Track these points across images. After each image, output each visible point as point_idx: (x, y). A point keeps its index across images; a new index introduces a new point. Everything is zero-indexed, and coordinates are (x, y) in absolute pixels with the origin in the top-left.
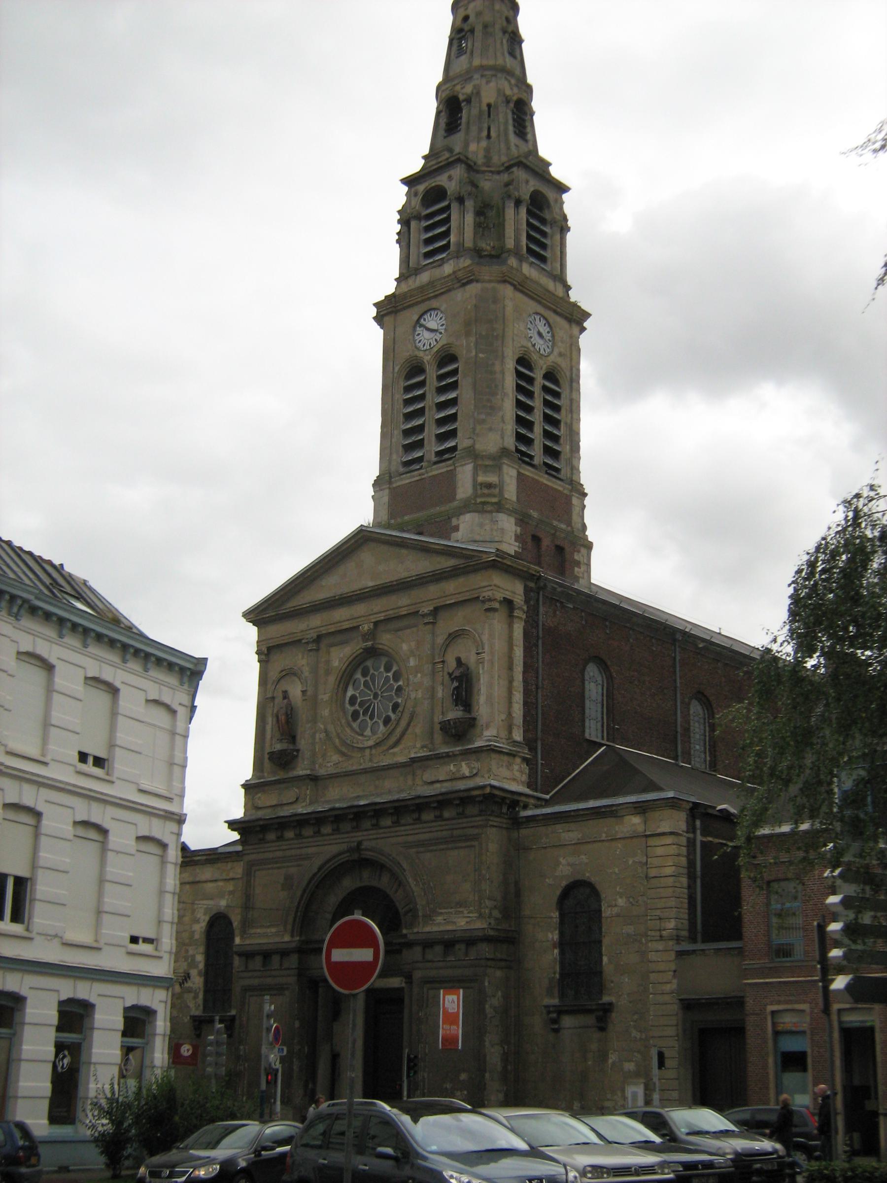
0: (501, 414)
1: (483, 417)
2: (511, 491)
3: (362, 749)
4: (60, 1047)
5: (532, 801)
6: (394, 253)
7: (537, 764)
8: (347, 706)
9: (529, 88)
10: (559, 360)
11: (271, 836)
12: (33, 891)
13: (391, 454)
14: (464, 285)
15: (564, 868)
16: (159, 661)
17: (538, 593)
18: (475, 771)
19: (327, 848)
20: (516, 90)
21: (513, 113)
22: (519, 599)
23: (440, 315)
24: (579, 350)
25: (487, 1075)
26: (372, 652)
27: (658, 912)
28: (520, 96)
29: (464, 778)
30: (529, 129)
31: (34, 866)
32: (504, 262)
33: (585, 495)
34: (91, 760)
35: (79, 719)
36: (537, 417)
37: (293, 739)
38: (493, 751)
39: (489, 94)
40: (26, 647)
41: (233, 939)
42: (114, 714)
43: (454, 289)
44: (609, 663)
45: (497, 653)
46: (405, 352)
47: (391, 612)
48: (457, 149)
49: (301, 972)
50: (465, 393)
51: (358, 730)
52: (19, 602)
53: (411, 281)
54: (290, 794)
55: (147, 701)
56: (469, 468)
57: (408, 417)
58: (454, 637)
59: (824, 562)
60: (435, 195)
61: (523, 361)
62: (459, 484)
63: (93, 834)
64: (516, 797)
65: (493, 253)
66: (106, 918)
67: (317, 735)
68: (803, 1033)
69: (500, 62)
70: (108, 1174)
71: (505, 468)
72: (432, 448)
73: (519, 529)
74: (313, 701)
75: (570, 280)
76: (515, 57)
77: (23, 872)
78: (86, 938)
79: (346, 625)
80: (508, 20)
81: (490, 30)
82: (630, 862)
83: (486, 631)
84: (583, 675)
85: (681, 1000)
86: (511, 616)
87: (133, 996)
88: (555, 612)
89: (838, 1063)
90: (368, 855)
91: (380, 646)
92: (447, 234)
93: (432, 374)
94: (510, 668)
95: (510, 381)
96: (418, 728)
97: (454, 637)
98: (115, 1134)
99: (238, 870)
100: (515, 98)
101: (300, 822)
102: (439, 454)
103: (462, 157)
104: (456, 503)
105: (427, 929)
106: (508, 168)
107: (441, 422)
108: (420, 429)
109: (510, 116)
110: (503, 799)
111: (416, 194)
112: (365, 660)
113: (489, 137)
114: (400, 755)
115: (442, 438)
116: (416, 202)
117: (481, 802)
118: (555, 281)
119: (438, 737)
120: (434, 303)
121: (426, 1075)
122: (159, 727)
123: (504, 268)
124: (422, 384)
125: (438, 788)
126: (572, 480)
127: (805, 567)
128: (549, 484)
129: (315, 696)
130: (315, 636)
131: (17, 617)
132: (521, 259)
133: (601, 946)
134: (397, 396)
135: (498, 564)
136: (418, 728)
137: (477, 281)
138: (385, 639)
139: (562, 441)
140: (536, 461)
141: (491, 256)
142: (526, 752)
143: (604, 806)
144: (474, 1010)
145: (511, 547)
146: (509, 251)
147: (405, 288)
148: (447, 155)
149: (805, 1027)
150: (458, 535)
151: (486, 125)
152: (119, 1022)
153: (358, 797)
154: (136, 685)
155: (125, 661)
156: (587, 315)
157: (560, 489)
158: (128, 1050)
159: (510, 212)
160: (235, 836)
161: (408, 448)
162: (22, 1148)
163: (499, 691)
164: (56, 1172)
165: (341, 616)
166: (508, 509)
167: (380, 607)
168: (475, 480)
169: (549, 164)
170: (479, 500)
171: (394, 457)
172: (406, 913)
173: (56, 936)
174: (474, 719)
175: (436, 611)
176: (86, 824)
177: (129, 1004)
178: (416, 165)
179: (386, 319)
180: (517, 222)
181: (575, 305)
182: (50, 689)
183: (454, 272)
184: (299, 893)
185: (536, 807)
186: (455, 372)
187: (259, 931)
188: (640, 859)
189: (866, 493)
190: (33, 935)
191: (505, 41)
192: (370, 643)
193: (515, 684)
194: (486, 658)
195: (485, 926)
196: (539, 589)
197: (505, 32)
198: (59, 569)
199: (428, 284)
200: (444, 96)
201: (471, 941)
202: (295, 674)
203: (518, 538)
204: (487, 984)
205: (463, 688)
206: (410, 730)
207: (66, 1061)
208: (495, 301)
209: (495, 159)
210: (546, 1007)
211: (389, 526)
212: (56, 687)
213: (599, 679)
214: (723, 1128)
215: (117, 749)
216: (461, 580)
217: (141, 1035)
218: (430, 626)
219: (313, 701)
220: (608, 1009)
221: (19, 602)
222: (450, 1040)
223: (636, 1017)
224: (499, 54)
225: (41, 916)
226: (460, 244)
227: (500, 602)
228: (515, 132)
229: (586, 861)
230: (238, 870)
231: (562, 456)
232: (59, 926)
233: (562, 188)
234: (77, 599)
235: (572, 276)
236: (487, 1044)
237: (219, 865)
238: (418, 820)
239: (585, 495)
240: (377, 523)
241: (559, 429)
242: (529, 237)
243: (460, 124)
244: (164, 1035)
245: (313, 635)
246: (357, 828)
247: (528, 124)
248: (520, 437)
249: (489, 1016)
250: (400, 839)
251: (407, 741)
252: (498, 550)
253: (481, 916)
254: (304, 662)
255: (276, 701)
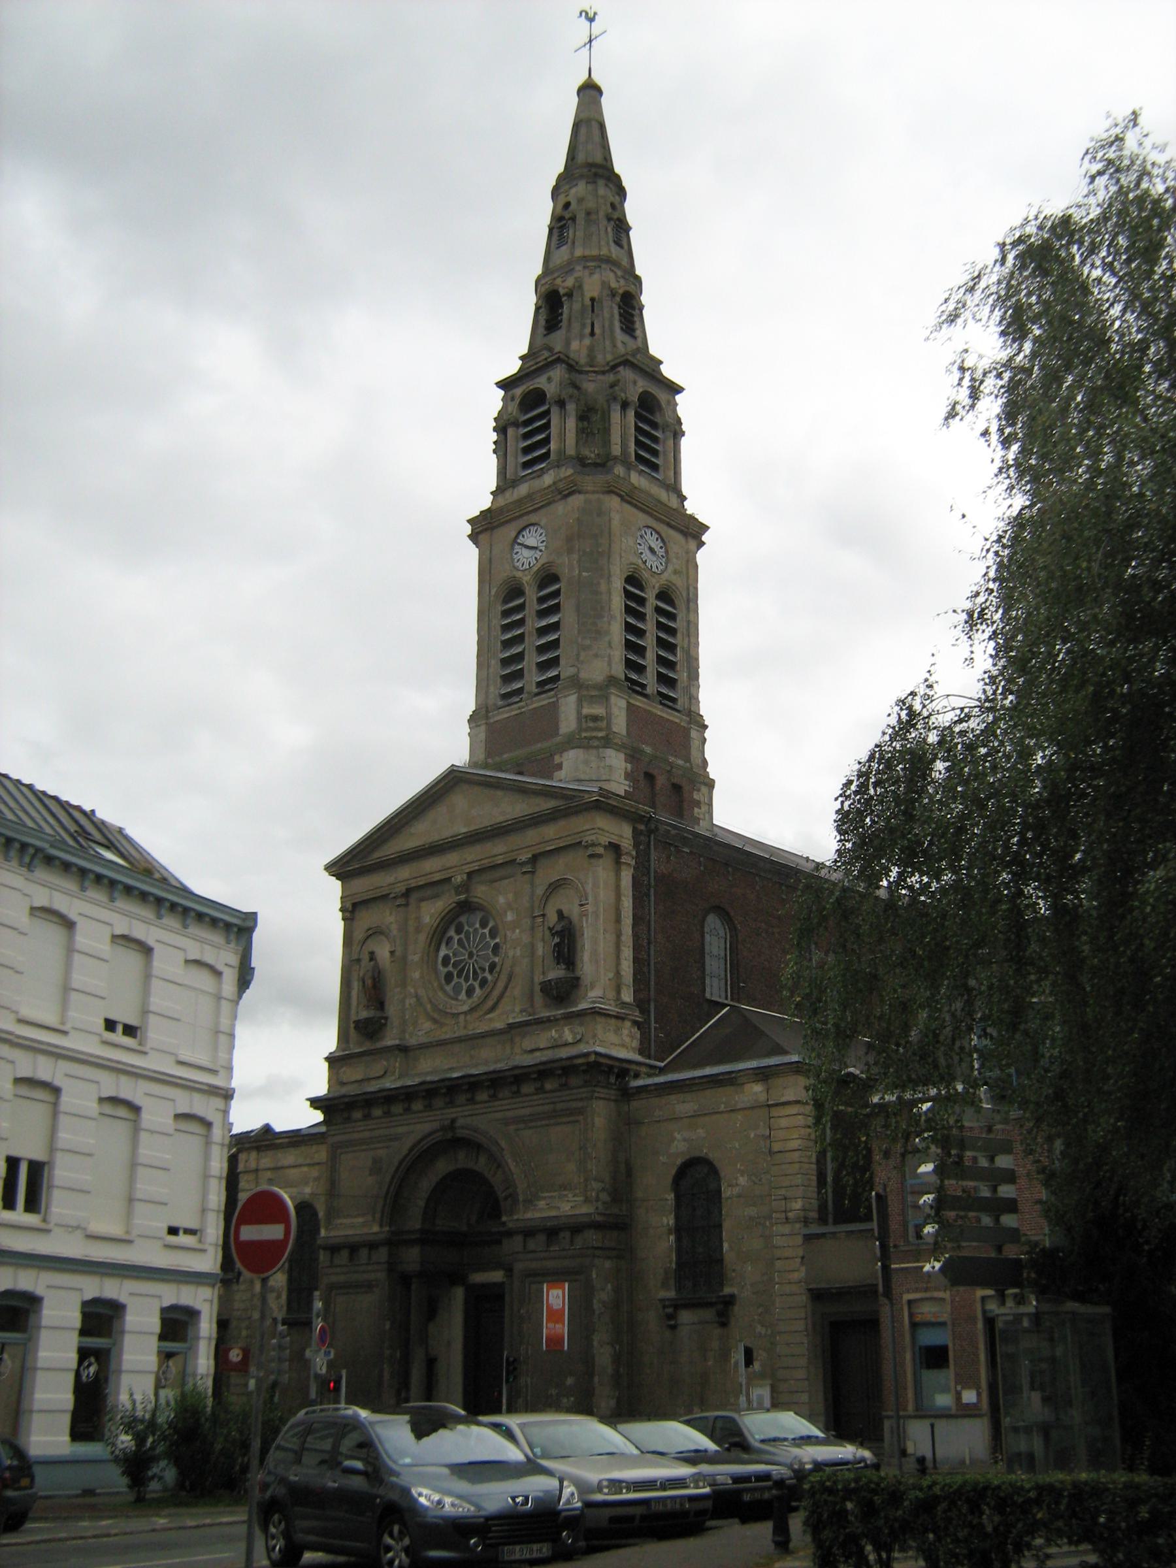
0: (607, 639)
1: (588, 642)
2: (620, 724)
3: (456, 1016)
4: (84, 1354)
5: (644, 1069)
6: (491, 463)
7: (649, 1028)
8: (440, 967)
9: (638, 279)
10: (676, 579)
11: (357, 1115)
12: (51, 1177)
13: (488, 686)
14: (566, 496)
15: (679, 1144)
16: (200, 916)
17: (649, 837)
18: (578, 1037)
19: (417, 1127)
20: (622, 282)
21: (620, 307)
22: (627, 843)
23: (540, 531)
24: (697, 566)
25: (596, 1379)
26: (465, 907)
27: (783, 1192)
28: (628, 289)
29: (566, 1045)
30: (637, 325)
31: (52, 1149)
32: (609, 471)
33: (706, 727)
34: (120, 1028)
35: (106, 982)
36: (649, 642)
37: (381, 1005)
38: (599, 1013)
39: (592, 286)
40: (41, 900)
41: (318, 1231)
42: (147, 976)
43: (554, 501)
44: (732, 914)
45: (603, 904)
46: (502, 573)
47: (486, 861)
48: (558, 348)
49: (391, 1267)
50: (568, 616)
51: (452, 994)
52: (31, 851)
53: (508, 494)
54: (378, 1068)
55: (187, 962)
56: (573, 699)
57: (507, 644)
58: (555, 887)
59: (878, 772)
60: (534, 399)
61: (633, 580)
62: (562, 716)
63: (122, 1112)
64: (625, 1065)
65: (598, 461)
66: (139, 1207)
67: (407, 1002)
68: (943, 1324)
69: (604, 252)
70: (131, 1497)
71: (613, 699)
72: (533, 677)
73: (629, 766)
74: (401, 961)
75: (685, 490)
76: (621, 246)
77: (38, 1155)
78: (115, 1229)
79: (437, 877)
80: (613, 206)
81: (594, 217)
82: (752, 1135)
83: (590, 881)
84: (703, 927)
85: (809, 1290)
86: (618, 863)
87: (171, 1295)
88: (668, 857)
89: (982, 1357)
90: (461, 1133)
91: (475, 900)
92: (547, 441)
93: (531, 595)
94: (618, 920)
95: (617, 602)
96: (517, 990)
97: (555, 887)
98: (136, 1453)
99: (321, 1153)
100: (621, 291)
101: (389, 1098)
102: (540, 684)
103: (562, 356)
104: (558, 739)
105: (529, 1215)
106: (614, 368)
107: (541, 649)
108: (520, 657)
109: (616, 311)
110: (611, 1067)
111: (513, 399)
112: (458, 916)
113: (592, 334)
114: (498, 1022)
115: (543, 666)
116: (513, 407)
117: (584, 1072)
118: (667, 490)
119: (539, 999)
120: (533, 518)
121: (529, 1380)
122: (203, 991)
123: (609, 477)
124: (521, 608)
125: (539, 1057)
126: (690, 711)
127: (855, 778)
128: (664, 715)
129: (404, 958)
130: (403, 889)
131: (30, 867)
132: (629, 467)
133: (721, 1232)
134: (494, 622)
135: (604, 804)
136: (517, 990)
137: (580, 492)
138: (481, 892)
139: (678, 667)
140: (649, 691)
141: (596, 465)
142: (637, 1015)
143: (722, 1074)
144: (581, 1306)
145: (620, 786)
146: (616, 458)
147: (501, 501)
148: (546, 354)
149: (945, 1317)
150: (562, 774)
151: (589, 321)
152: (154, 1323)
153: (451, 1069)
154: (172, 943)
155: (159, 917)
156: (705, 528)
157: (677, 721)
158: (166, 1356)
159: (616, 416)
160: (318, 1116)
161: (507, 679)
162: (10, 1468)
163: (605, 945)
164: (77, 1496)
165: (432, 866)
166: (616, 744)
167: (473, 856)
168: (579, 713)
169: (661, 362)
170: (584, 734)
171: (492, 689)
172: (506, 1198)
173: (78, 1227)
174: (578, 979)
175: (535, 859)
176: (115, 1101)
177: (166, 1304)
178: (512, 367)
179: (481, 537)
180: (624, 427)
181: (692, 518)
182: (70, 949)
183: (554, 483)
184: (388, 1179)
185: (649, 1075)
186: (557, 593)
187: (345, 1221)
188: (761, 1131)
189: (922, 690)
190: (50, 1226)
191: (609, 229)
192: (463, 897)
193: (623, 938)
194: (590, 910)
195: (591, 1210)
196: (650, 832)
197: (609, 219)
198: (90, 815)
199: (525, 497)
200: (543, 289)
201: (576, 1228)
202: (381, 933)
203: (628, 776)
204: (594, 1276)
205: (565, 942)
206: (507, 994)
207: (92, 1370)
208: (600, 514)
209: (600, 358)
210: (661, 1300)
211: (486, 766)
212: (78, 946)
213: (722, 933)
214: (805, 1433)
215: (151, 1016)
216: (562, 823)
217: (184, 1339)
218: (527, 876)
219: (401, 961)
220: (730, 1301)
221: (31, 851)
222: (555, 1341)
223: (760, 1310)
224: (603, 243)
225: (59, 1205)
226: (562, 452)
227: (605, 847)
228: (622, 329)
229: (704, 1135)
230: (321, 1153)
231: (679, 684)
232: (84, 1213)
233: (676, 389)
234: (107, 848)
235: (687, 486)
236: (595, 1343)
237: (303, 1148)
238: (517, 1093)
239: (706, 727)
240: (473, 763)
241: (675, 655)
242: (638, 443)
243: (561, 321)
244: (210, 1339)
245: (401, 888)
246: (451, 1103)
247: (636, 319)
248: (630, 664)
249: (597, 1312)
250: (499, 1115)
251: (506, 1004)
252: (601, 789)
253: (587, 1200)
254: (392, 919)
255: (363, 963)
